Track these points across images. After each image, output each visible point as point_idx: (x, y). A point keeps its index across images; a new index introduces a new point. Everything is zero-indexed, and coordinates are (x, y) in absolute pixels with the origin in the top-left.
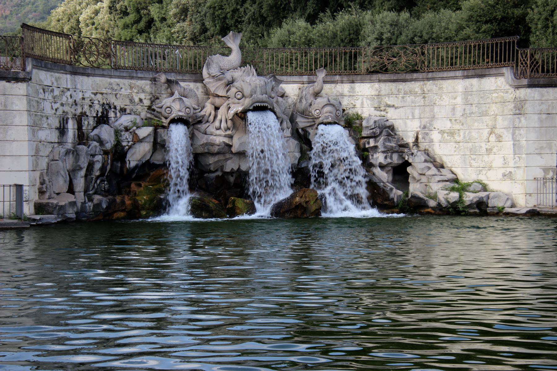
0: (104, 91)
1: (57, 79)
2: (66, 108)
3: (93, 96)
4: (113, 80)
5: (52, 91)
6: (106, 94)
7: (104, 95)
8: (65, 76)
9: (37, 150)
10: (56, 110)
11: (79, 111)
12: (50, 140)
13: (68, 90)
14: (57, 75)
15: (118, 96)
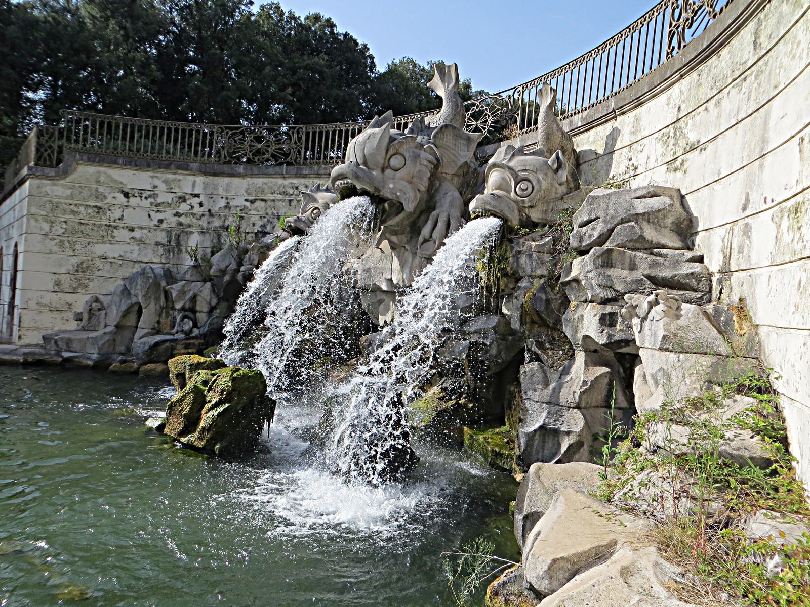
0: (270, 197)
1: (165, 182)
2: (182, 219)
3: (248, 204)
4: (287, 182)
5: (155, 196)
6: (274, 200)
7: (269, 203)
8: (192, 178)
9: (81, 268)
10: (161, 221)
11: (217, 223)
12: (134, 257)
13: (198, 196)
14: (171, 176)
15: (294, 203)
